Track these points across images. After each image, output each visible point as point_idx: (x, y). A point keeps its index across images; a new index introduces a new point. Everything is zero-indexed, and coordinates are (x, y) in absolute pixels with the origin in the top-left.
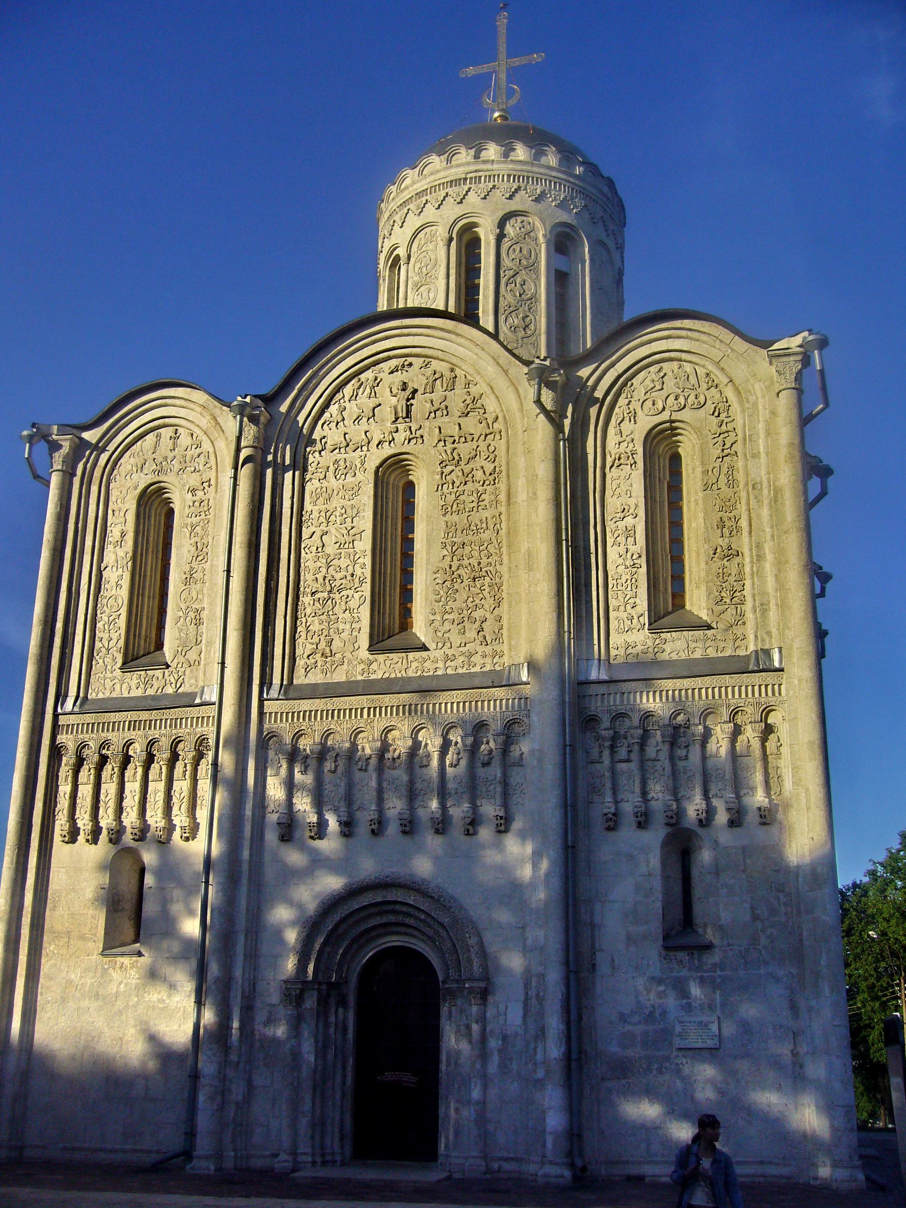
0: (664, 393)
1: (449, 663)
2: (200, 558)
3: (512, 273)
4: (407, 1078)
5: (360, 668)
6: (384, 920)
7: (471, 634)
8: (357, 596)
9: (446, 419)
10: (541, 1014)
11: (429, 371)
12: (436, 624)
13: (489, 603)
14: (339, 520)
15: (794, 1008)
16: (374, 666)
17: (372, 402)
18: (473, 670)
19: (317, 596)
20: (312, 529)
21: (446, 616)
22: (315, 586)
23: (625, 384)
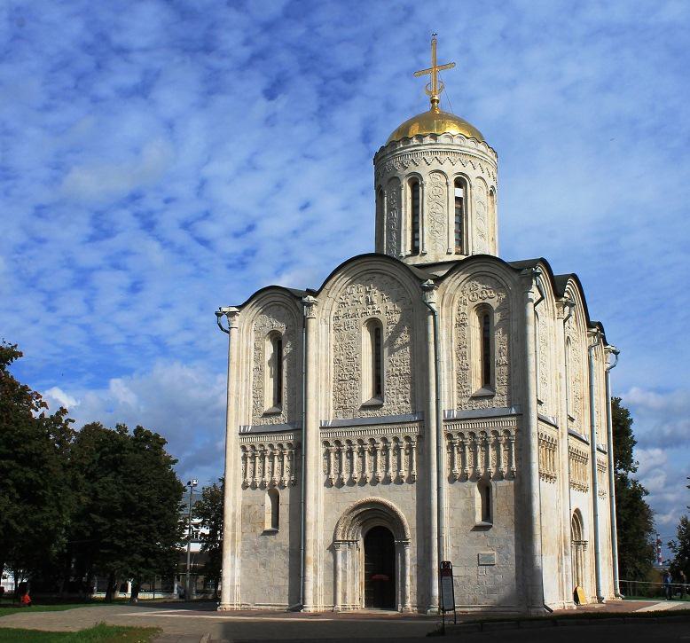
4: (385, 577)
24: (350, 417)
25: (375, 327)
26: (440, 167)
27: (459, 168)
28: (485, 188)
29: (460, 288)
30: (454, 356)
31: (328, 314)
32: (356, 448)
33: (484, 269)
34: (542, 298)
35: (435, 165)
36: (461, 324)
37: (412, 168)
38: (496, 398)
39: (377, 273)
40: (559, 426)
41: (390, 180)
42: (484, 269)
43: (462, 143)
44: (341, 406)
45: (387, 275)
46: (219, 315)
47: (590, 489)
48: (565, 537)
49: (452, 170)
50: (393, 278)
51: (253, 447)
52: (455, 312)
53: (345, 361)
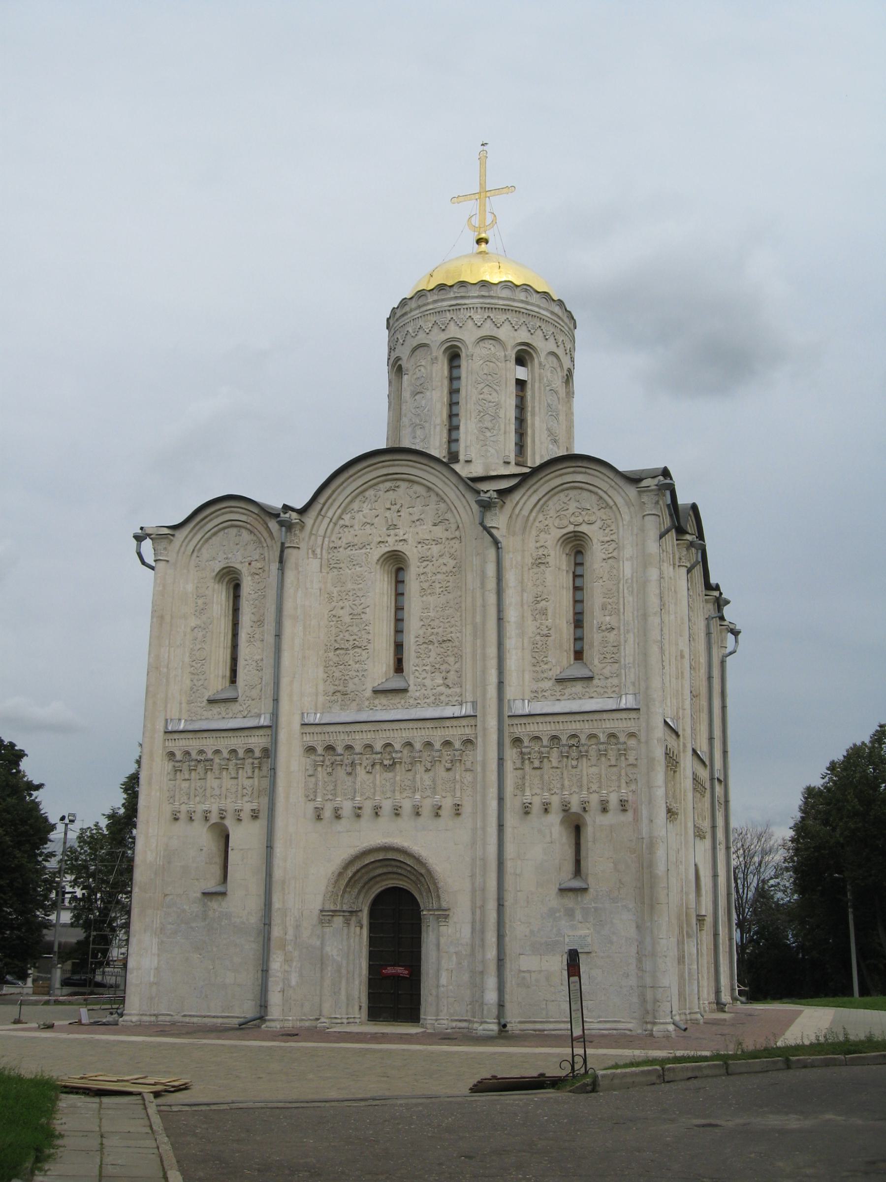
0: (571, 511)
3: (482, 385)
4: (401, 971)
5: (367, 703)
6: (385, 870)
7: (441, 682)
8: (364, 653)
9: (425, 527)
10: (483, 931)
11: (411, 492)
12: (417, 674)
13: (451, 660)
14: (351, 598)
15: (638, 927)
16: (377, 702)
17: (374, 512)
19: (338, 652)
20: (334, 604)
21: (425, 668)
22: (337, 646)
23: (543, 505)
25: (396, 564)
26: (495, 332)
27: (523, 336)
28: (559, 370)
31: (320, 540)
33: (579, 478)
35: (488, 329)
36: (540, 562)
37: (453, 331)
38: (595, 682)
40: (680, 733)
41: (414, 350)
42: (579, 478)
43: (529, 299)
44: (341, 694)
46: (139, 538)
47: (709, 836)
48: (687, 908)
49: (512, 336)
50: (429, 489)
51: (187, 753)
52: (532, 545)
53: (347, 619)
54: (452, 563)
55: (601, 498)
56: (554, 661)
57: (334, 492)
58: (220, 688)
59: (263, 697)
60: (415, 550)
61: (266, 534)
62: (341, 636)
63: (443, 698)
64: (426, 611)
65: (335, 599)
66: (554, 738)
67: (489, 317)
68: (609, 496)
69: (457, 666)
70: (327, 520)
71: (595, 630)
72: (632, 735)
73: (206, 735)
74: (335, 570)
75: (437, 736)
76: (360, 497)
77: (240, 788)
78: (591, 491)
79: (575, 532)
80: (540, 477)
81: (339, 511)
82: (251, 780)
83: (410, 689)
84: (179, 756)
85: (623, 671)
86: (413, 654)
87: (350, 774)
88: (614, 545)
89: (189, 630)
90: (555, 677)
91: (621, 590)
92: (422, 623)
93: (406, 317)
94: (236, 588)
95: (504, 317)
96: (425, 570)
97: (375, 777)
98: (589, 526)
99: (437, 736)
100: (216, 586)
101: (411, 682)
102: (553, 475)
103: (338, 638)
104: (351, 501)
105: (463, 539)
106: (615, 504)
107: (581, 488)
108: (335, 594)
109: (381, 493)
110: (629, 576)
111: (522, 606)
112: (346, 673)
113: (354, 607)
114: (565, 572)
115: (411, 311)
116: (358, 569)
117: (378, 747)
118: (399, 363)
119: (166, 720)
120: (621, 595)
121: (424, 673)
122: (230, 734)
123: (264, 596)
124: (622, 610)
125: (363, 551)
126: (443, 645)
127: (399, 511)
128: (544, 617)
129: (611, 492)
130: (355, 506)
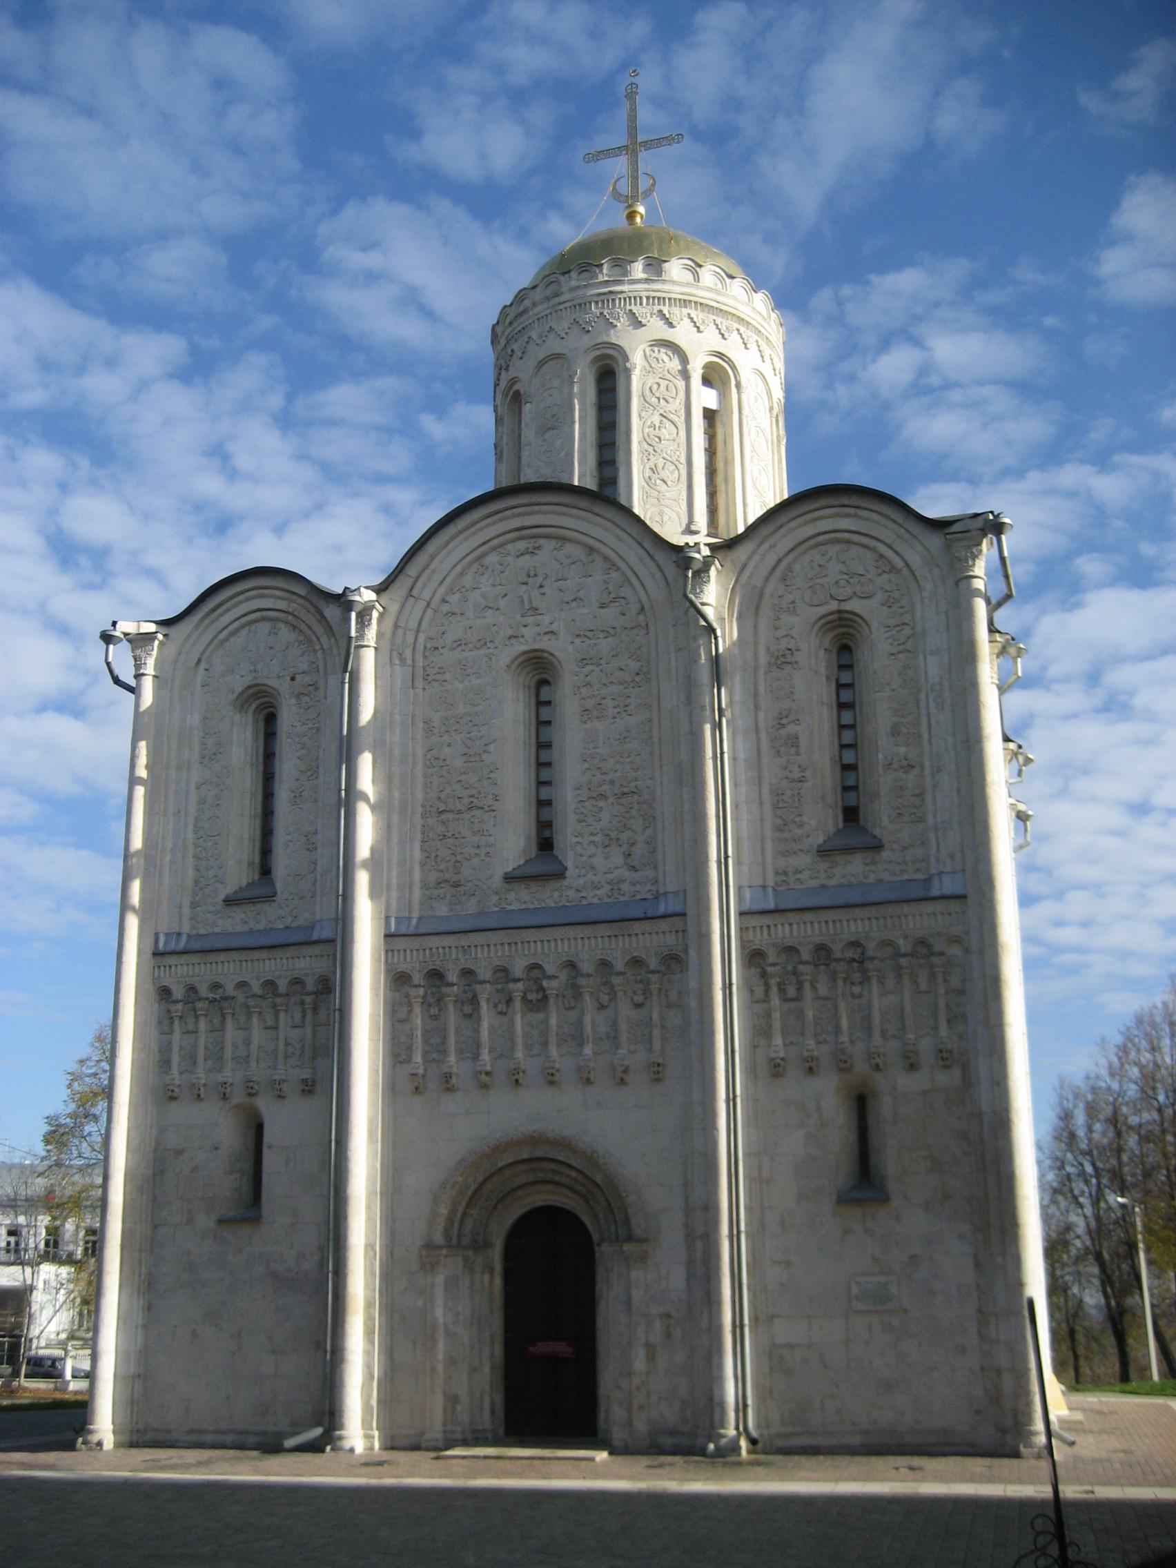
1: (596, 892)
2: (309, 773)
5: (494, 899)
7: (617, 858)
9: (585, 611)
12: (578, 847)
13: (638, 824)
15: (978, 1265)
16: (511, 896)
18: (622, 899)
19: (444, 817)
21: (593, 838)
24: (471, 907)
25: (539, 672)
26: (669, 334)
29: (778, 573)
30: (765, 745)
31: (410, 638)
32: (484, 992)
33: (844, 524)
34: (1009, 596)
38: (886, 854)
39: (547, 537)
41: (542, 363)
42: (844, 524)
45: (570, 540)
51: (192, 989)
53: (459, 763)
54: (634, 665)
55: (882, 556)
56: (813, 822)
57: (433, 557)
58: (244, 883)
59: (318, 893)
60: (570, 648)
61: (319, 629)
62: (448, 791)
63: (625, 887)
64: (591, 745)
65: (436, 731)
66: (822, 951)
67: (660, 311)
68: (897, 553)
69: (648, 832)
70: (422, 604)
71: (881, 770)
72: (955, 940)
73: (222, 957)
74: (436, 684)
75: (619, 950)
76: (476, 566)
77: (281, 1044)
78: (865, 546)
79: (840, 612)
80: (779, 523)
81: (442, 589)
82: (298, 1031)
83: (568, 874)
84: (178, 993)
85: (932, 836)
86: (572, 818)
87: (469, 1016)
88: (907, 631)
89: (193, 787)
90: (815, 848)
91: (923, 704)
92: (586, 765)
93: (525, 317)
94: (269, 722)
95: (685, 311)
96: (588, 679)
97: (512, 1021)
98: (863, 602)
99: (619, 950)
100: (237, 717)
101: (569, 864)
102: (801, 520)
103: (443, 796)
104: (461, 574)
105: (652, 629)
106: (907, 565)
107: (848, 542)
108: (436, 723)
109: (510, 559)
110: (937, 679)
111: (757, 731)
112: (459, 850)
113: (469, 742)
114: (824, 679)
115: (534, 305)
116: (475, 682)
117: (518, 969)
118: (515, 388)
119: (157, 935)
120: (923, 711)
121: (592, 847)
122: (264, 954)
123: (318, 730)
124: (926, 736)
125: (483, 651)
126: (623, 801)
127: (541, 586)
128: (793, 751)
129: (897, 546)
130: (468, 580)
